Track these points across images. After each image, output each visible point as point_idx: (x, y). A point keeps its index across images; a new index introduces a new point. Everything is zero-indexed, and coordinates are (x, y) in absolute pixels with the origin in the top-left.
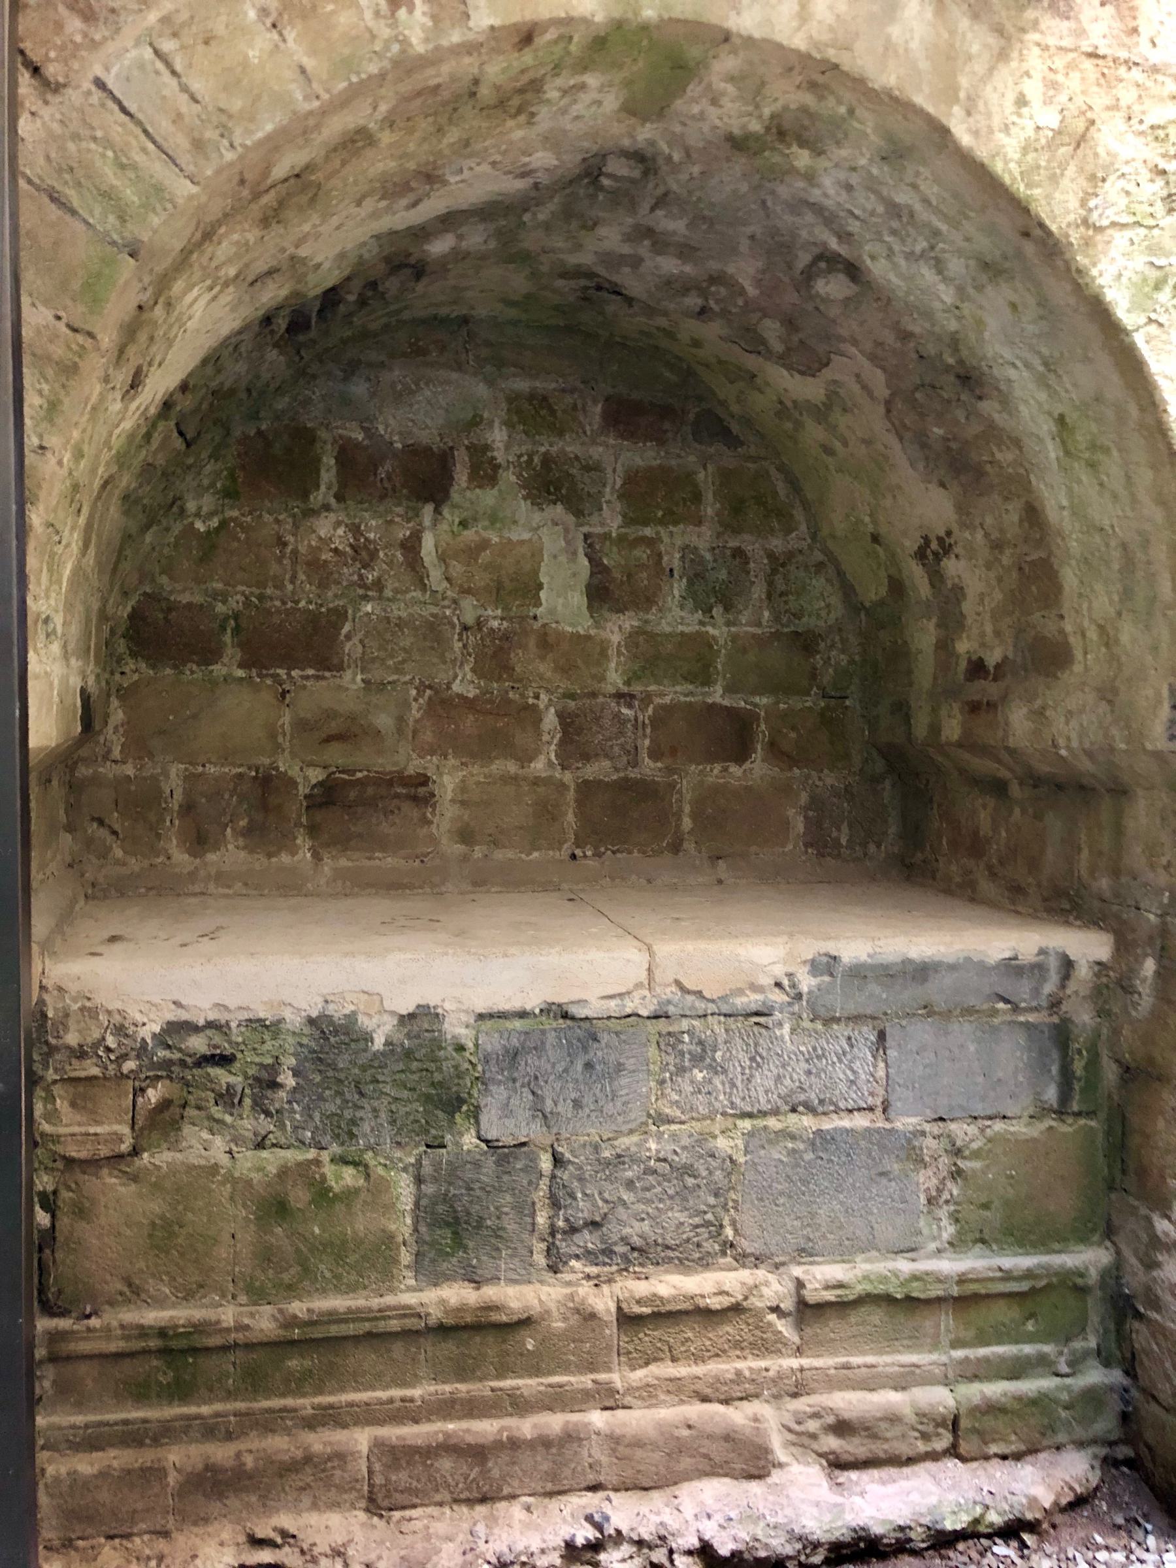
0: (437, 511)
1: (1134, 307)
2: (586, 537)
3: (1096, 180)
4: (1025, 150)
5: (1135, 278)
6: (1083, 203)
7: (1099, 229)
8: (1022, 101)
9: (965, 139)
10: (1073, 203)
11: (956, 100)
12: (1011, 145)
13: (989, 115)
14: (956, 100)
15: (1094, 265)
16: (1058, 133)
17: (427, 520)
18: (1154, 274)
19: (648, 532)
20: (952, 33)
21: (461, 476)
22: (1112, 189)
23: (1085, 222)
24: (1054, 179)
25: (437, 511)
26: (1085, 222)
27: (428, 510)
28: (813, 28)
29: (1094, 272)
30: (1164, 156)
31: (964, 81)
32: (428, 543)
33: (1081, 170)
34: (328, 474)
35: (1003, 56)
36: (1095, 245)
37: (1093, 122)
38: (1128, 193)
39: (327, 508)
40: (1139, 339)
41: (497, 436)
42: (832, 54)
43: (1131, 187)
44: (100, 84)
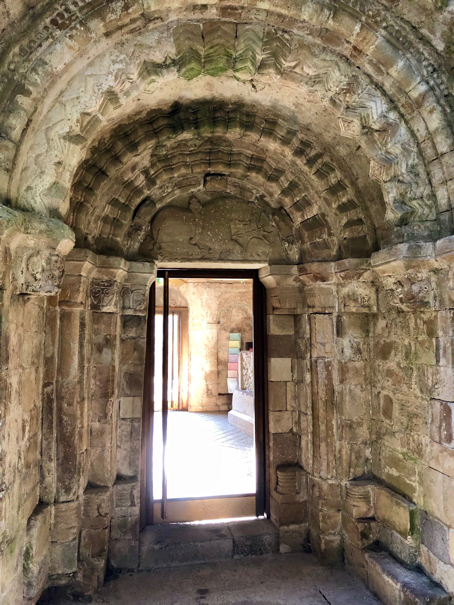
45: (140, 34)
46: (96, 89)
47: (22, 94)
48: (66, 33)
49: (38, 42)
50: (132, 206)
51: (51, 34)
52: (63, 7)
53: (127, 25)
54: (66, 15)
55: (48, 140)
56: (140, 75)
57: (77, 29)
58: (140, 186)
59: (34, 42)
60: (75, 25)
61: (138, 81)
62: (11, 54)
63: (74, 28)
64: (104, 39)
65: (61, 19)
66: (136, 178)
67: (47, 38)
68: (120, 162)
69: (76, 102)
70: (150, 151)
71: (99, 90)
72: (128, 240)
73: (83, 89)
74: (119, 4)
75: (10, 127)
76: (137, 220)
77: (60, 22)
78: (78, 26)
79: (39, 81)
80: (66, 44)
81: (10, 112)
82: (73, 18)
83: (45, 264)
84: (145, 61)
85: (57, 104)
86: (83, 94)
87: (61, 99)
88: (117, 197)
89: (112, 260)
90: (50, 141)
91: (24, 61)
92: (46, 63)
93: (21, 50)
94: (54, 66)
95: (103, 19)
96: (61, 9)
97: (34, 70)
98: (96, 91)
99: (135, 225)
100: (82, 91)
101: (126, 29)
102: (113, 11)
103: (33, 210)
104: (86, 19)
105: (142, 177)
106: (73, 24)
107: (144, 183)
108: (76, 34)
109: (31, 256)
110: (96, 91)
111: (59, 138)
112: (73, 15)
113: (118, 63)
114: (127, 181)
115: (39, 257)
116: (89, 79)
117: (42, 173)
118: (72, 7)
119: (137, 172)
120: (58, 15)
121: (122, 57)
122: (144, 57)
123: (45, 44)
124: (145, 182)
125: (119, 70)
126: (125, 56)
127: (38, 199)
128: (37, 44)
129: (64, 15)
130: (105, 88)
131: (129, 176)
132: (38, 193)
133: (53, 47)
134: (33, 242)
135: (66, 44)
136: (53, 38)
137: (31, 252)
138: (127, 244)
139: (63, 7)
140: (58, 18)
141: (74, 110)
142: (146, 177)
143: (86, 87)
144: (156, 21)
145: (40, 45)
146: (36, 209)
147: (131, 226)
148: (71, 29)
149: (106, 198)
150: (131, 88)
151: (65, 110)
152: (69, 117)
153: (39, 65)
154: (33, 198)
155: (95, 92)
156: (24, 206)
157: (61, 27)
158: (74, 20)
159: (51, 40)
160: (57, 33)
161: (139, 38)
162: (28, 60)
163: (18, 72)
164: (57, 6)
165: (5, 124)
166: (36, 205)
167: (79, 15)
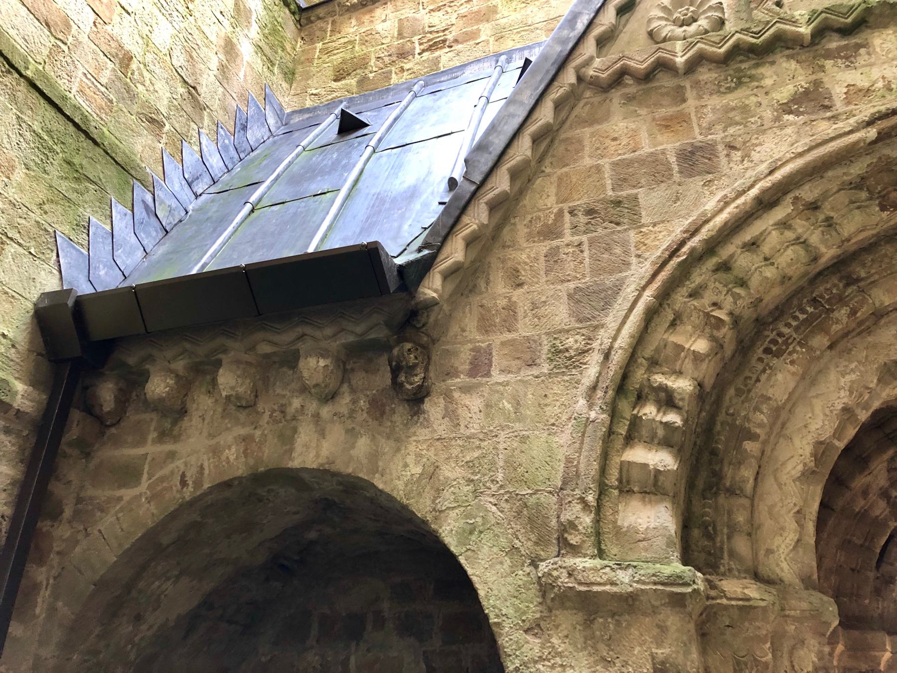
0: (357, 645)
1: (460, 543)
2: (424, 652)
3: (438, 490)
4: (406, 485)
5: (459, 530)
6: (433, 502)
7: (441, 512)
8: (406, 465)
9: (381, 486)
10: (429, 502)
11: (377, 471)
12: (400, 484)
13: (391, 474)
14: (377, 471)
15: (441, 528)
16: (421, 474)
17: (353, 649)
18: (469, 527)
19: (454, 648)
20: (377, 447)
21: (369, 627)
22: (447, 494)
23: (434, 509)
24: (420, 494)
25: (357, 645)
26: (434, 509)
27: (354, 644)
28: (320, 461)
29: (441, 531)
30: (472, 473)
31: (380, 464)
32: (353, 660)
33: (432, 488)
34: (314, 632)
35: (398, 450)
36: (440, 519)
37: (437, 467)
38: (454, 493)
39: (312, 647)
40: (462, 560)
41: (385, 605)
42: (327, 467)
43: (457, 491)
44: (100, 531)
45: (869, 333)
46: (827, 412)
47: (750, 439)
48: (785, 360)
49: (754, 377)
50: (876, 548)
51: (768, 364)
52: (775, 333)
53: (853, 330)
54: (780, 340)
55: (780, 485)
56: (879, 380)
57: (797, 352)
58: (881, 517)
59: (750, 378)
60: (794, 347)
61: (878, 388)
62: (727, 398)
63: (794, 351)
64: (828, 352)
65: (775, 345)
66: (871, 507)
67: (764, 371)
68: (847, 487)
69: (804, 431)
70: (885, 464)
71: (831, 411)
72: (878, 601)
73: (810, 415)
74: (843, 312)
75: (744, 481)
76: (885, 568)
77: (774, 349)
78: (798, 348)
79: (765, 420)
80: (789, 371)
81: (740, 463)
82: (790, 341)
83: (815, 659)
84: (885, 364)
85: (781, 440)
86: (810, 420)
87: (784, 432)
88: (848, 537)
89: (869, 636)
90: (783, 487)
91: (743, 402)
92: (769, 399)
93: (737, 390)
94: (779, 399)
95: (827, 333)
96: (773, 335)
97: (757, 409)
98: (828, 412)
99: (883, 575)
100: (810, 418)
101: (854, 334)
102: (838, 321)
103: (781, 580)
104: (806, 338)
105: (882, 504)
106: (791, 348)
107: (887, 512)
108: (798, 358)
109: (794, 648)
110: (828, 412)
111: (794, 481)
112: (788, 339)
113: (849, 373)
114: (858, 513)
115: (805, 649)
116: (814, 401)
117: (783, 529)
118: (786, 330)
119: (872, 497)
120: (770, 342)
121: (853, 366)
122: (882, 359)
123: (764, 377)
124: (888, 510)
125: (852, 382)
126: (856, 363)
127: (784, 565)
128: (754, 379)
129: (778, 341)
130: (840, 407)
131: (860, 504)
132: (783, 557)
133: (773, 378)
134: (793, 627)
135: (789, 371)
136: (771, 368)
137: (791, 642)
138: (878, 608)
139: (775, 333)
140: (772, 346)
141: (805, 442)
142: (888, 503)
143: (813, 412)
144: (890, 314)
145: (758, 380)
146: (786, 580)
147: (877, 578)
148: (790, 354)
149: (835, 541)
150: (870, 398)
151: (793, 445)
152: (801, 452)
153: (762, 403)
154: (778, 565)
155: (827, 416)
156: (769, 576)
157: (778, 354)
158: (791, 343)
159: (768, 372)
160: (774, 362)
161: (870, 339)
162: (747, 400)
163: (739, 415)
164: (766, 333)
165: (737, 478)
166: (783, 574)
167: (795, 335)
